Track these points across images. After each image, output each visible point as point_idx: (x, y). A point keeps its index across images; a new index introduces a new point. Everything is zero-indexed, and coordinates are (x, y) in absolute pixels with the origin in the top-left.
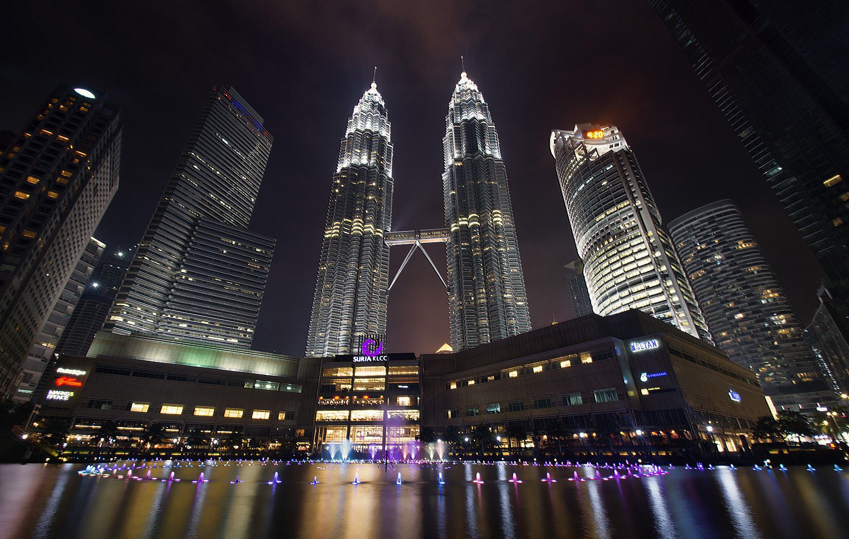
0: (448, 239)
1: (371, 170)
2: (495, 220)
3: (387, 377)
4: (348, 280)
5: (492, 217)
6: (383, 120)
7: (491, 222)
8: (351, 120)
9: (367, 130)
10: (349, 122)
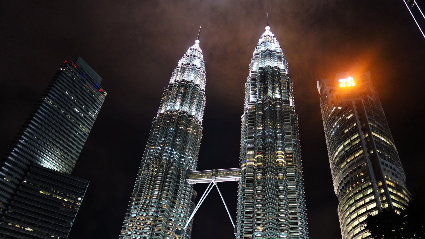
2: (277, 161)
5: (275, 158)
6: (199, 71)
9: (184, 80)
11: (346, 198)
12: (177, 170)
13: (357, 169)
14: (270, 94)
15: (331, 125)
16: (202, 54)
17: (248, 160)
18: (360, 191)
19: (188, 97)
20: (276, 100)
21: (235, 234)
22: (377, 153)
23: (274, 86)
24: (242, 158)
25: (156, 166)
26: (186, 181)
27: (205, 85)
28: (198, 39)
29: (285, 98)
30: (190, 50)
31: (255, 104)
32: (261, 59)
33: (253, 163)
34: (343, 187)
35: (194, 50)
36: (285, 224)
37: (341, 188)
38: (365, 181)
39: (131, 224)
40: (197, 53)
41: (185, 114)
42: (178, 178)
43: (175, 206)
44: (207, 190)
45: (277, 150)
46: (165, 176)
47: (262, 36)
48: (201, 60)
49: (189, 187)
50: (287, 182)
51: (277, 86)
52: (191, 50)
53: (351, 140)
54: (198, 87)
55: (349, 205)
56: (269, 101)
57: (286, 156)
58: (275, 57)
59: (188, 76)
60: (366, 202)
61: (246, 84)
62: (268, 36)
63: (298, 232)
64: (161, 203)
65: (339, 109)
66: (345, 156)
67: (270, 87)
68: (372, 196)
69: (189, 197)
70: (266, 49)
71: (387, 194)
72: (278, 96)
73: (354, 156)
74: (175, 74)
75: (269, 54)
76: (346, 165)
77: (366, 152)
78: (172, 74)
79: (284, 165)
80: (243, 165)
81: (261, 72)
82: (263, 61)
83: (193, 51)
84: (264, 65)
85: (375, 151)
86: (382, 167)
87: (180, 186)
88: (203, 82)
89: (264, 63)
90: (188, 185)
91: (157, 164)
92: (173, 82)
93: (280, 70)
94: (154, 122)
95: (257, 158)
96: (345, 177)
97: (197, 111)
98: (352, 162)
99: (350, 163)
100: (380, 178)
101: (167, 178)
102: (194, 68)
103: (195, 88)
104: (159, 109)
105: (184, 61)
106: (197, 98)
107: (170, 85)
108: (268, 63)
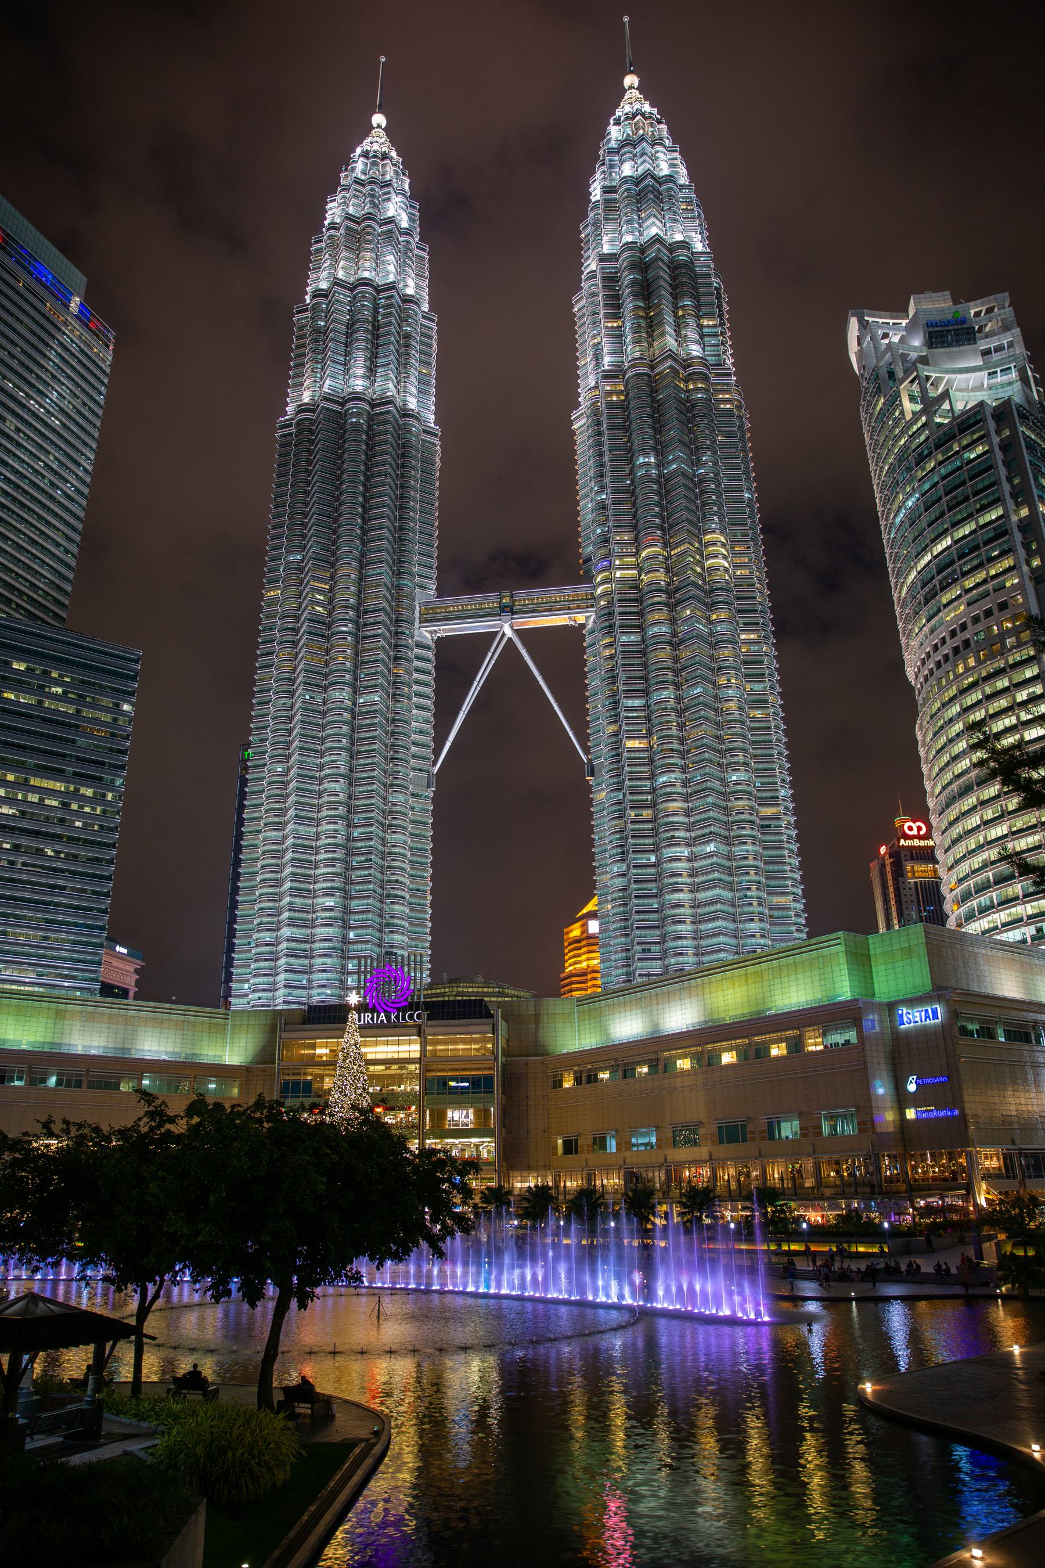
0: (587, 618)
1: (378, 410)
3: (419, 1061)
4: (328, 736)
5: (702, 556)
7: (699, 569)
9: (365, 282)
11: (954, 688)
13: (995, 611)
16: (404, 174)
20: (690, 365)
23: (680, 313)
28: (381, 111)
33: (635, 572)
35: (375, 156)
39: (280, 770)
44: (490, 654)
45: (706, 532)
51: (689, 314)
52: (368, 158)
54: (415, 307)
56: (671, 367)
57: (732, 548)
60: (1019, 699)
63: (773, 766)
72: (695, 350)
73: (988, 573)
74: (327, 256)
82: (636, 217)
83: (374, 164)
89: (639, 224)
93: (693, 253)
94: (282, 436)
95: (648, 558)
96: (955, 629)
98: (981, 589)
102: (390, 230)
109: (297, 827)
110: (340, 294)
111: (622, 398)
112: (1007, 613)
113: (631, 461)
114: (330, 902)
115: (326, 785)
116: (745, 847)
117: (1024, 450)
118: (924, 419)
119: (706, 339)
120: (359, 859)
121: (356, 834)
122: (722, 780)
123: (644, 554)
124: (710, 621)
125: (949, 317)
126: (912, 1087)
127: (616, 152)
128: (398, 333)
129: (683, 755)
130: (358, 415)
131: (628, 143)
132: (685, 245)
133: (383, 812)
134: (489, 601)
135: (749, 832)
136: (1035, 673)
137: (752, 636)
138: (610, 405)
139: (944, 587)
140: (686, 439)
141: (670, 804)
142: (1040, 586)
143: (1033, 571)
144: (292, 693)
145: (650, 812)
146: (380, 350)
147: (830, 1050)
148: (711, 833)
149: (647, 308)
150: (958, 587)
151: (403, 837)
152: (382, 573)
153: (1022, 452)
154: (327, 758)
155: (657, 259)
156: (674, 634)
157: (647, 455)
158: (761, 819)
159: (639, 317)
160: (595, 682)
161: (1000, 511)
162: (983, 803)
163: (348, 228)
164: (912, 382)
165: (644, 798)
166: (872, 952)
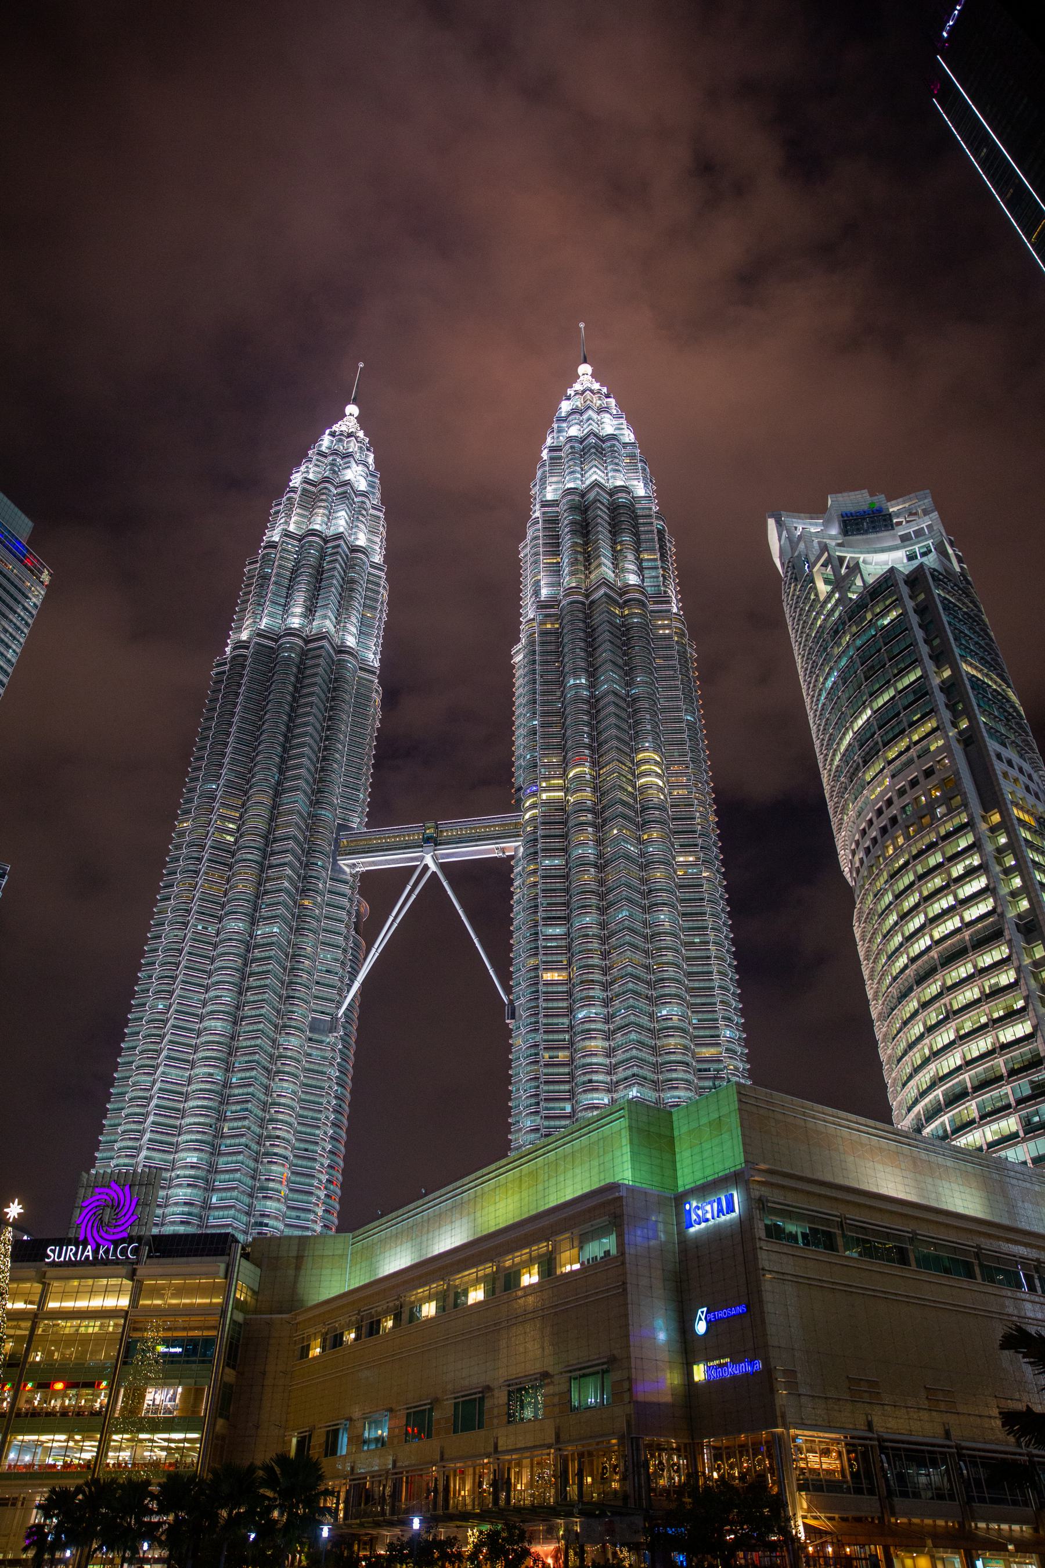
5: (633, 774)
6: (363, 502)
8: (277, 508)
9: (313, 533)
10: (272, 511)
11: (885, 873)
12: (307, 826)
13: (921, 779)
14: (607, 571)
15: (829, 650)
16: (368, 450)
17: (544, 784)
18: (932, 846)
19: (331, 585)
20: (626, 593)
21: (508, 1021)
22: (982, 726)
23: (619, 548)
24: (520, 778)
25: (233, 814)
26: (335, 862)
27: (384, 552)
28: (355, 402)
29: (655, 586)
30: (331, 438)
31: (559, 605)
32: (571, 463)
34: (875, 841)
36: (674, 979)
37: (868, 843)
38: (950, 810)
39: (161, 1007)
40: (353, 446)
41: (325, 643)
42: (309, 853)
43: (305, 942)
44: (409, 888)
45: (637, 751)
46: (267, 845)
47: (570, 392)
48: (366, 469)
49: (346, 882)
50: (673, 847)
53: (896, 689)
54: (363, 556)
55: (897, 892)
56: (606, 594)
58: (615, 457)
59: (326, 519)
60: (955, 875)
61: (522, 545)
62: (588, 392)
63: (713, 1000)
64: (259, 932)
65: (851, 599)
66: (880, 743)
67: (605, 550)
68: (971, 855)
69: (349, 913)
70: (585, 432)
71: (1013, 846)
72: (633, 579)
73: (910, 739)
74: (283, 515)
75: (596, 446)
76: (884, 768)
77: (948, 725)
78: (271, 515)
79: (662, 797)
80: (527, 804)
81: (573, 508)
82: (579, 469)
83: (340, 440)
84: (582, 480)
85: (972, 719)
86: (999, 767)
87: (318, 879)
88: (378, 540)
89: (582, 475)
90: (344, 877)
91: (234, 808)
92: (276, 539)
93: (633, 497)
94: (217, 674)
95: (576, 777)
96: (881, 808)
97: (362, 636)
98: (903, 758)
99: (897, 762)
100: (991, 798)
101: (273, 854)
102: (346, 492)
103: (353, 558)
104: (231, 629)
105: (311, 471)
106: (361, 590)
107: (265, 548)
108: (595, 475)
109: (168, 1070)
110: (288, 544)
111: (557, 626)
112: (934, 780)
113: (562, 684)
114: (193, 1158)
115: (206, 1024)
116: (676, 1093)
117: (941, 611)
118: (837, 595)
119: (647, 573)
120: (234, 1108)
121: (234, 1080)
122: (651, 1015)
123: (571, 775)
124: (640, 841)
125: (865, 508)
126: (701, 1328)
127: (564, 420)
128: (343, 579)
129: (606, 986)
130: (291, 649)
131: (574, 411)
132: (625, 489)
133: (271, 1056)
134: (413, 832)
135: (681, 1075)
136: (970, 842)
137: (691, 859)
138: (544, 633)
139: (866, 761)
140: (620, 662)
141: (587, 1043)
142: (969, 748)
143: (961, 733)
144: (185, 924)
145: (567, 1053)
146: (321, 592)
147: (590, 1268)
148: (634, 1075)
149: (586, 543)
150: (881, 760)
151: (292, 1086)
152: (297, 801)
153: (939, 613)
154: (212, 994)
155: (596, 500)
156: (600, 855)
157: (577, 677)
158: (698, 1061)
159: (577, 552)
160: (519, 916)
161: (919, 673)
162: (925, 1005)
163: (304, 490)
164: (824, 565)
165: (561, 1037)
166: (676, 1133)
